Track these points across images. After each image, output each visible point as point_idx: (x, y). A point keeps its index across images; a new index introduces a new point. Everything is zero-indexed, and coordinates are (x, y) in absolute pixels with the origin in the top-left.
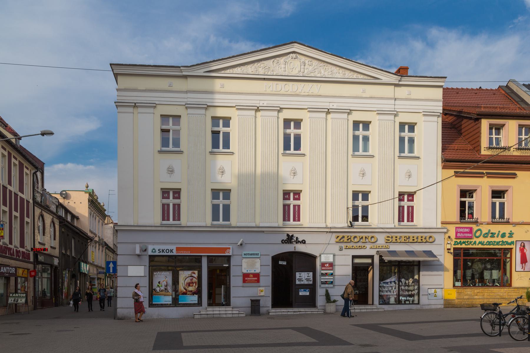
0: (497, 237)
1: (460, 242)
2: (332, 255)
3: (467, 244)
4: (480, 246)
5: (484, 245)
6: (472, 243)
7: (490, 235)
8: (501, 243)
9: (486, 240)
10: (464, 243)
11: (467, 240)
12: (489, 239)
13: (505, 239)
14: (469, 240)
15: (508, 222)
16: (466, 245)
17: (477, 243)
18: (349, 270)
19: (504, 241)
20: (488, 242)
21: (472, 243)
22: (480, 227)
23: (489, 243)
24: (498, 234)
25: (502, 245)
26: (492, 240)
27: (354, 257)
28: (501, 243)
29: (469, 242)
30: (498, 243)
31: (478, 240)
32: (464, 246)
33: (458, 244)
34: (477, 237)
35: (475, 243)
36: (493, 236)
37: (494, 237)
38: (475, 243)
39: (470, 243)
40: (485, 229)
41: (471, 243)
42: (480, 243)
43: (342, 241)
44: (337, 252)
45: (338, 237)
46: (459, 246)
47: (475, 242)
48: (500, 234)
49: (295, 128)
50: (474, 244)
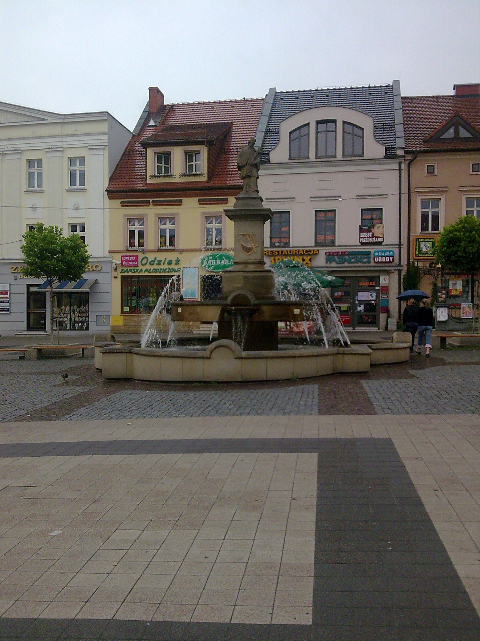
0: (164, 264)
1: (127, 269)
2: (9, 284)
3: (133, 271)
4: (147, 274)
5: (151, 272)
6: (139, 271)
7: (156, 262)
8: (167, 270)
9: (152, 268)
10: (131, 270)
11: (133, 268)
12: (156, 267)
13: (171, 267)
14: (136, 268)
15: (174, 250)
16: (132, 272)
17: (143, 271)
18: (24, 298)
19: (171, 268)
20: (154, 269)
21: (139, 271)
22: (147, 255)
23: (156, 271)
24: (165, 261)
25: (168, 272)
27: (29, 286)
28: (167, 270)
29: (135, 270)
30: (164, 271)
32: (130, 274)
33: (124, 272)
34: (143, 265)
35: (141, 270)
36: (159, 264)
37: (160, 264)
38: (141, 270)
39: (137, 270)
40: (151, 257)
41: (137, 270)
42: (146, 270)
43: (16, 271)
44: (13, 282)
45: (13, 267)
46: (126, 274)
47: (142, 269)
48: (167, 261)
50: (140, 271)
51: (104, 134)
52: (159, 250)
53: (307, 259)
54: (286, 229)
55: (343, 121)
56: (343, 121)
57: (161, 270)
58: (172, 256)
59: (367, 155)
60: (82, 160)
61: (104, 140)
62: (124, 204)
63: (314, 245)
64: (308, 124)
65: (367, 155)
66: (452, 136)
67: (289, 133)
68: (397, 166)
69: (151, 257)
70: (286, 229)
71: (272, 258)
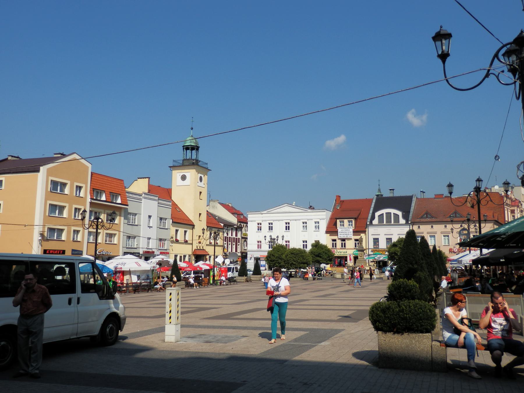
4: (337, 255)
9: (339, 254)
12: (340, 253)
15: (345, 249)
22: (337, 250)
26: (341, 254)
31: (336, 254)
34: (336, 253)
49: (288, 224)
51: (325, 215)
52: (341, 249)
53: (384, 252)
54: (378, 243)
55: (393, 213)
56: (393, 213)
57: (342, 254)
58: (345, 250)
59: (400, 223)
60: (318, 223)
61: (324, 217)
62: (330, 235)
63: (386, 248)
64: (383, 214)
65: (400, 223)
66: (426, 217)
67: (379, 216)
68: (409, 226)
69: (339, 250)
70: (378, 243)
71: (374, 252)
